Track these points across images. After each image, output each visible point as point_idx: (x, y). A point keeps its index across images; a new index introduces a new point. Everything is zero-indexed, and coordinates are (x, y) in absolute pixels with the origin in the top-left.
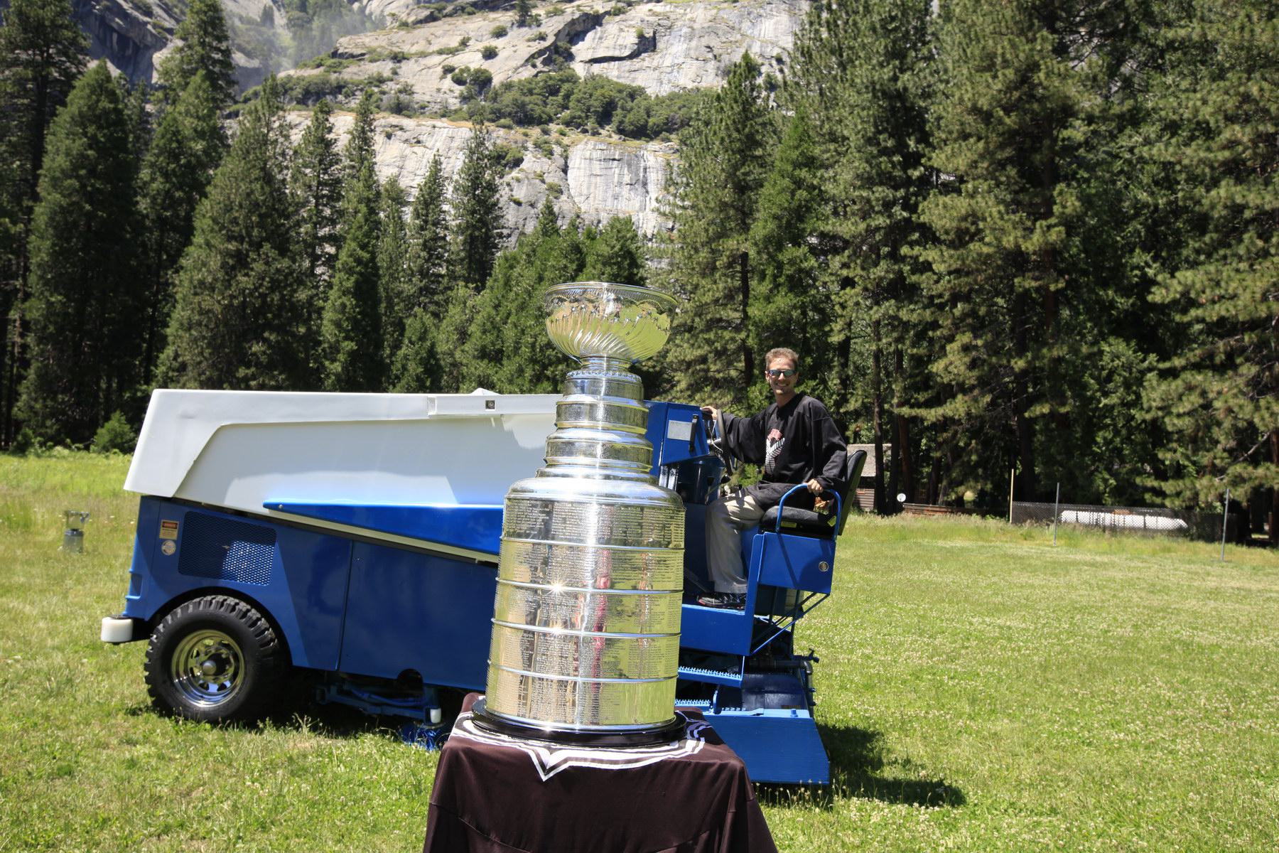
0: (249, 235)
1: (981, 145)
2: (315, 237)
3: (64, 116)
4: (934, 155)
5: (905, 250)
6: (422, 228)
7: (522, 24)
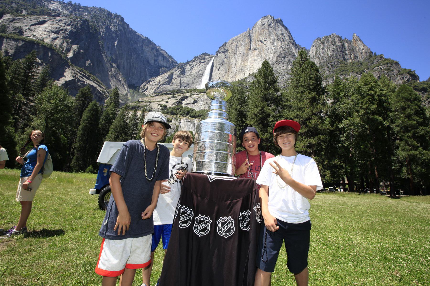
0: (120, 132)
1: (255, 120)
2: (132, 132)
3: (87, 109)
7: (173, 97)
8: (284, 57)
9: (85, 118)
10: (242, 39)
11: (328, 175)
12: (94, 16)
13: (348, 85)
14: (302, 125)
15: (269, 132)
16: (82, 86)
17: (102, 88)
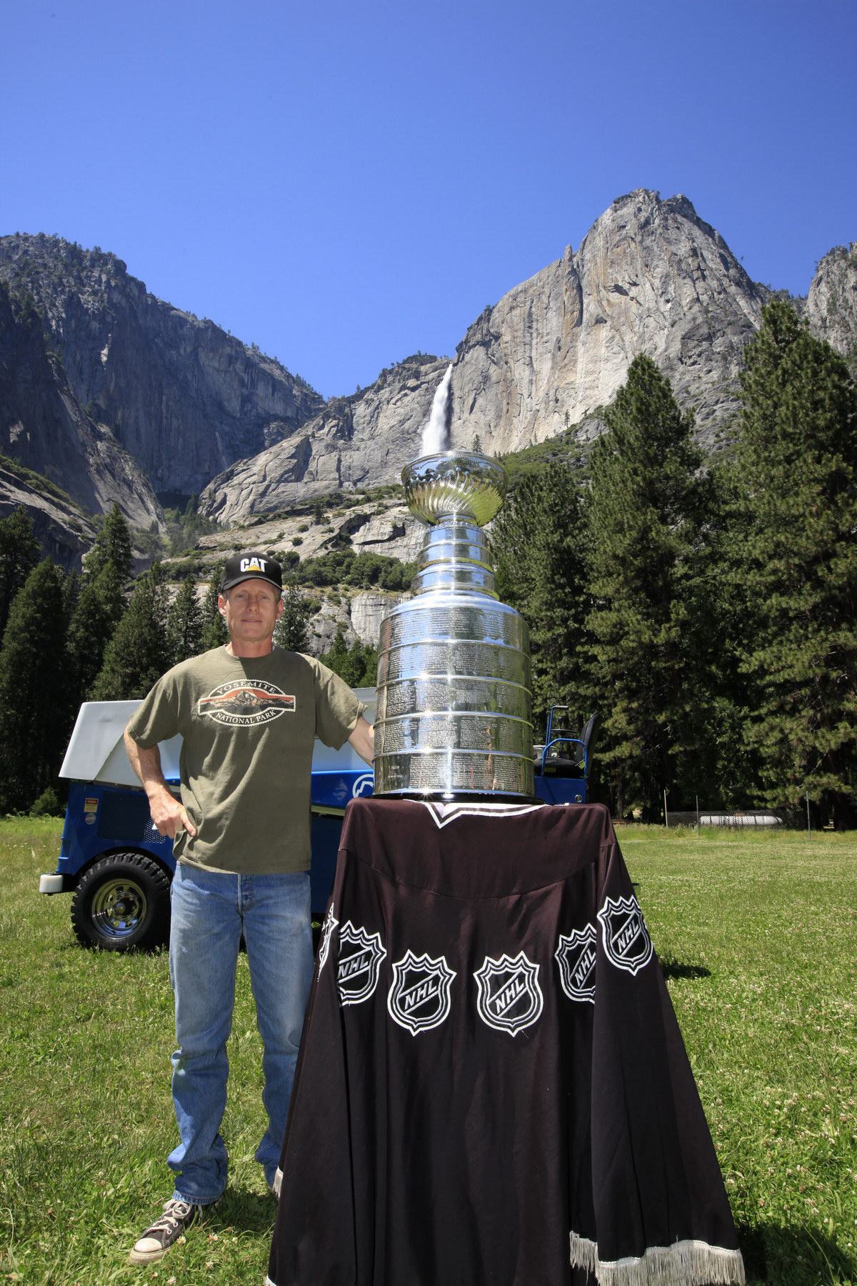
0: (140, 662)
1: (621, 578)
3: (23, 593)
4: (591, 587)
5: (579, 648)
7: (318, 523)
8: (710, 338)
9: (20, 622)
10: (547, 290)
12: (24, 268)
14: (799, 581)
15: (677, 620)
17: (69, 513)
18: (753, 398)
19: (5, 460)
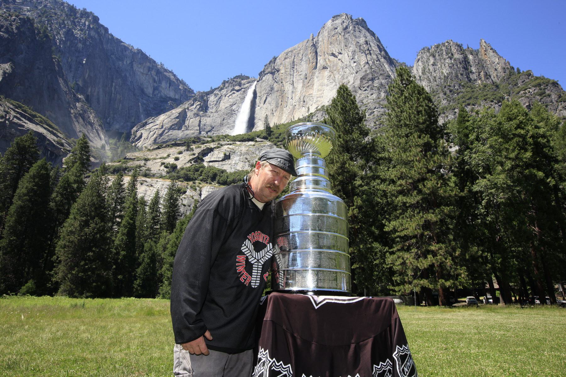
3: (27, 176)
6: (152, 213)
7: (187, 150)
8: (373, 80)
9: (24, 191)
10: (301, 52)
11: (463, 276)
13: (480, 121)
15: (357, 206)
16: (18, 133)
17: (57, 136)
18: (392, 108)
19: (23, 107)
